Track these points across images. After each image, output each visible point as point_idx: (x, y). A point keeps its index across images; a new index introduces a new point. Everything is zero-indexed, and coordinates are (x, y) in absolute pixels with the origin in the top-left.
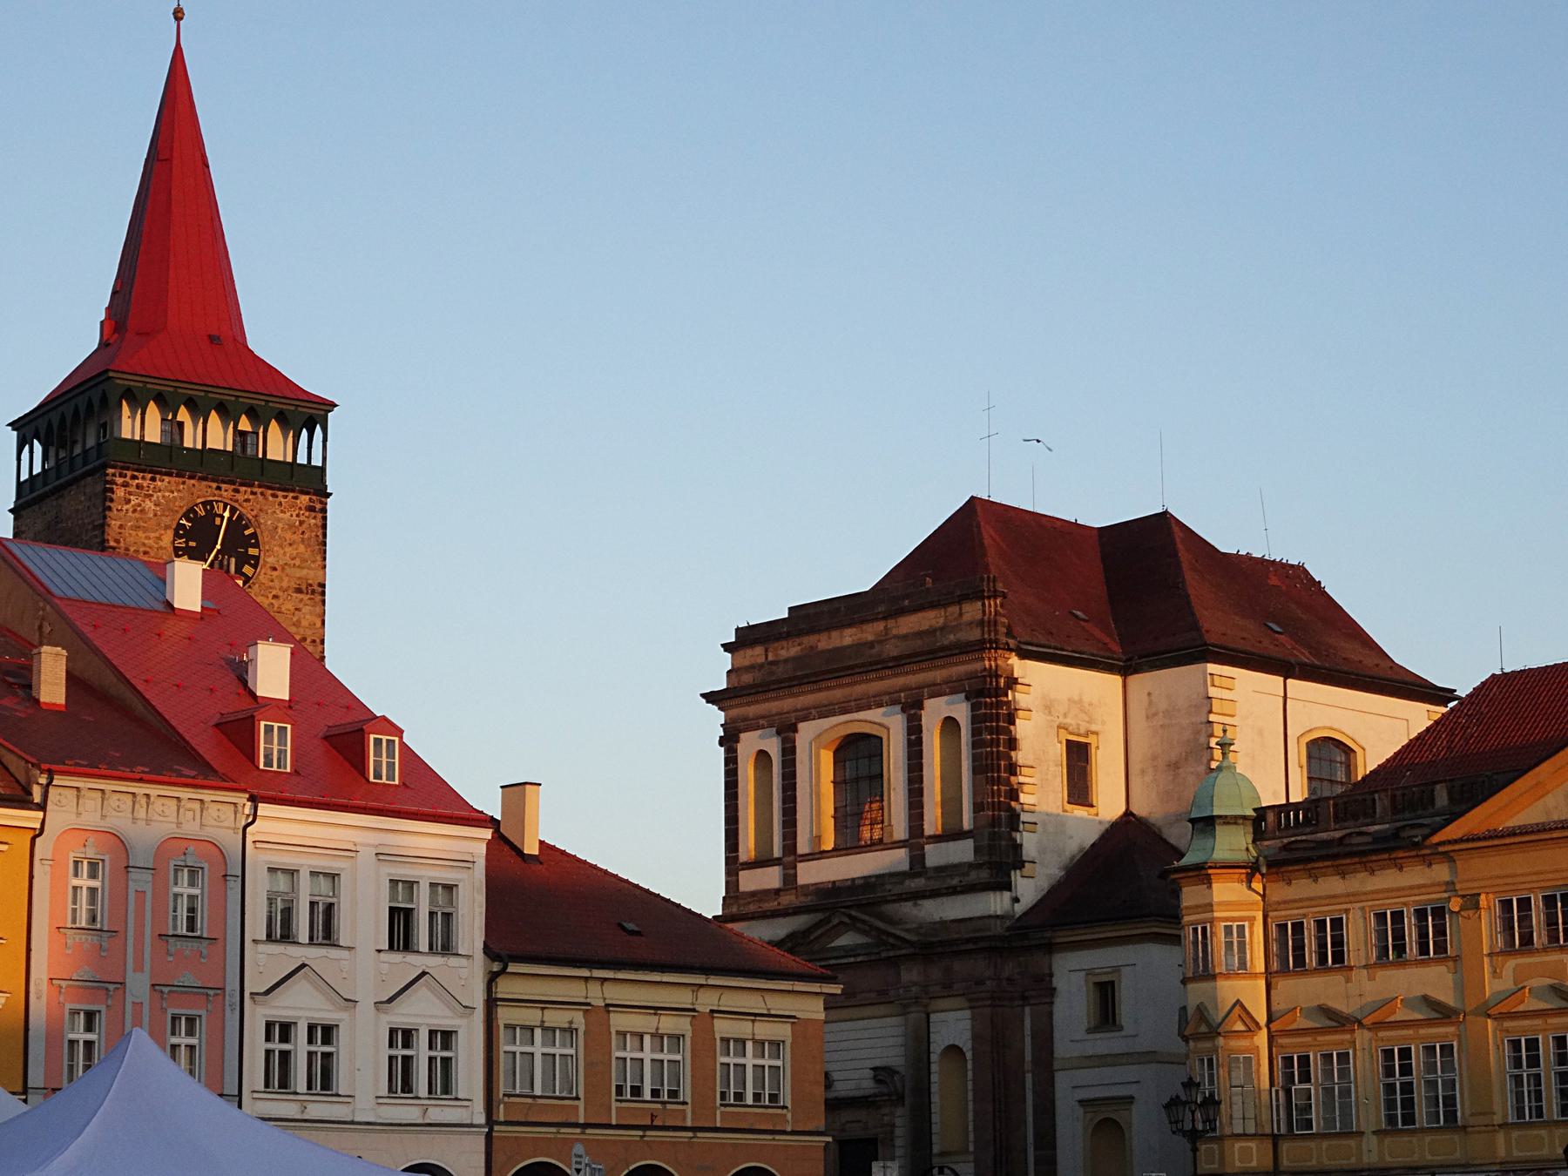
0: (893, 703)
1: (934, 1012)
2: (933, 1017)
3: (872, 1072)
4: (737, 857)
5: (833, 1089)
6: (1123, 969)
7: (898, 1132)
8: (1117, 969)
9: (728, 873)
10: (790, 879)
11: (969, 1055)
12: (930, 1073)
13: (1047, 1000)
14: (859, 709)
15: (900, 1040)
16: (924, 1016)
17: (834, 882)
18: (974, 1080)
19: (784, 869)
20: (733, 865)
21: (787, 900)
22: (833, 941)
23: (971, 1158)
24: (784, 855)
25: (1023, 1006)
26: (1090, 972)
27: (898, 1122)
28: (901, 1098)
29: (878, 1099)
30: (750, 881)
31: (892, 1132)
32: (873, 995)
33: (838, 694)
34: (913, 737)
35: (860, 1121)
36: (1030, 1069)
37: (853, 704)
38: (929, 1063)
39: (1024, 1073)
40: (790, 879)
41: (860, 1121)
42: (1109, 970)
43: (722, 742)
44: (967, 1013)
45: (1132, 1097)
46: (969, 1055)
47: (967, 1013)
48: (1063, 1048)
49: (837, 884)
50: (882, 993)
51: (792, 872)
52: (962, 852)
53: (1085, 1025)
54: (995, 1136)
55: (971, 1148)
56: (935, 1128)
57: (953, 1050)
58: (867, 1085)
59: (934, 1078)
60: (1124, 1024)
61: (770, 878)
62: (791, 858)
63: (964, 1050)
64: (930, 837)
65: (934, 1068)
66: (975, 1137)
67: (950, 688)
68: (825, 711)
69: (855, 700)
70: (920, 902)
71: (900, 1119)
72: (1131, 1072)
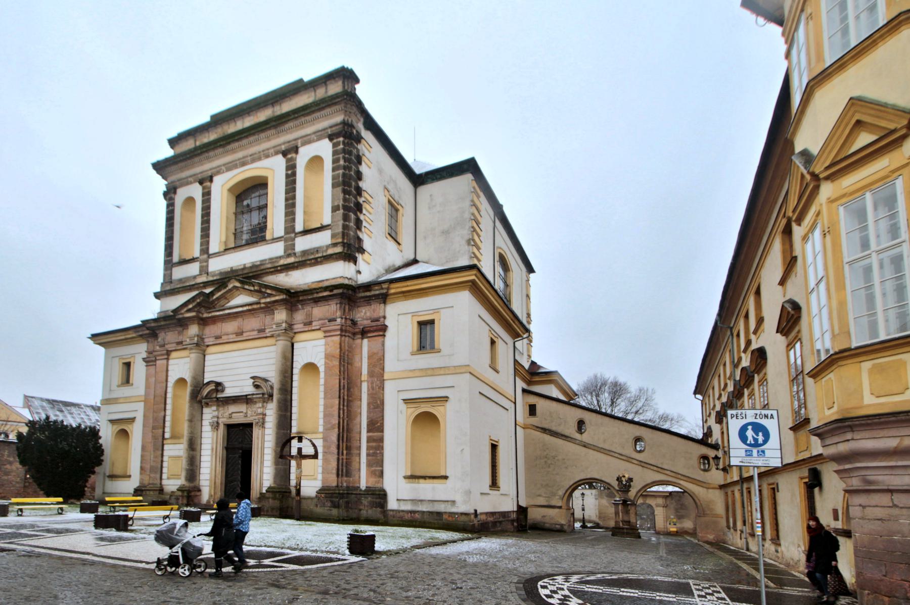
0: (277, 153)
1: (297, 342)
2: (296, 346)
3: (252, 381)
4: (172, 259)
5: (225, 393)
6: (442, 311)
7: (268, 419)
8: (436, 311)
9: (166, 269)
10: (204, 270)
11: (322, 369)
12: (292, 381)
13: (381, 333)
14: (253, 161)
15: (273, 361)
16: (290, 344)
17: (232, 268)
18: (325, 384)
19: (200, 263)
20: (169, 264)
21: (203, 279)
22: (229, 301)
23: (321, 436)
24: (201, 255)
25: (362, 339)
26: (414, 314)
27: (268, 412)
28: (271, 396)
29: (254, 396)
30: (179, 273)
31: (263, 419)
32: (256, 333)
33: (240, 155)
34: (290, 172)
35: (242, 412)
36: (366, 379)
37: (249, 158)
38: (292, 374)
39: (361, 381)
40: (204, 270)
41: (242, 412)
42: (431, 312)
43: (165, 194)
44: (323, 342)
45: (447, 397)
46: (322, 369)
47: (323, 342)
48: (391, 365)
49: (234, 269)
50: (261, 331)
51: (205, 264)
52: (323, 239)
53: (411, 350)
54: (339, 422)
55: (321, 429)
56: (294, 417)
57: (311, 367)
58: (247, 388)
59: (295, 384)
60: (441, 347)
61: (193, 269)
62: (205, 256)
63: (318, 365)
64: (300, 233)
65: (295, 377)
66: (324, 422)
67: (316, 136)
68: (230, 167)
69: (251, 156)
70: (290, 273)
71: (271, 411)
72: (448, 380)
